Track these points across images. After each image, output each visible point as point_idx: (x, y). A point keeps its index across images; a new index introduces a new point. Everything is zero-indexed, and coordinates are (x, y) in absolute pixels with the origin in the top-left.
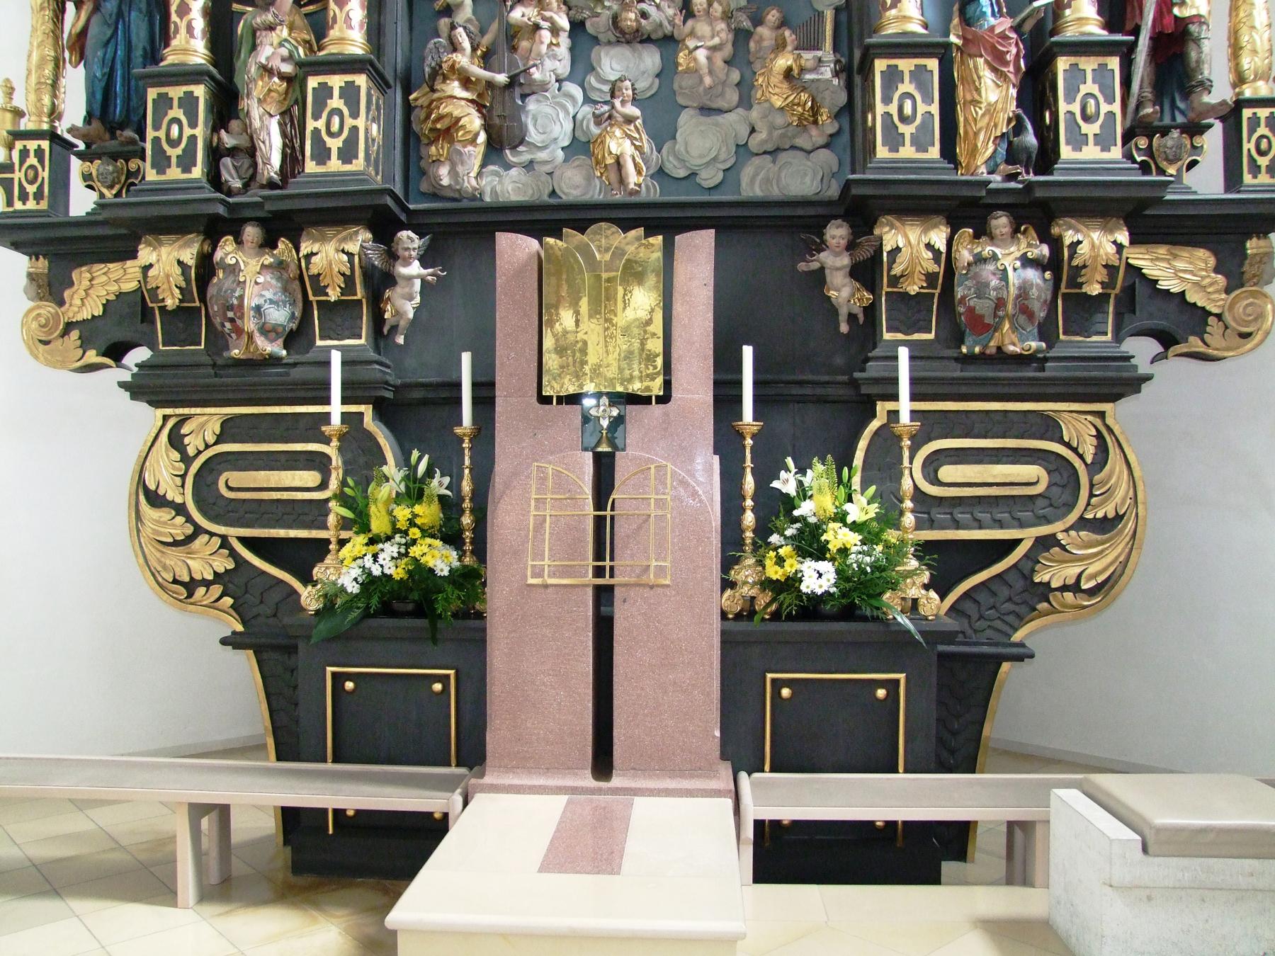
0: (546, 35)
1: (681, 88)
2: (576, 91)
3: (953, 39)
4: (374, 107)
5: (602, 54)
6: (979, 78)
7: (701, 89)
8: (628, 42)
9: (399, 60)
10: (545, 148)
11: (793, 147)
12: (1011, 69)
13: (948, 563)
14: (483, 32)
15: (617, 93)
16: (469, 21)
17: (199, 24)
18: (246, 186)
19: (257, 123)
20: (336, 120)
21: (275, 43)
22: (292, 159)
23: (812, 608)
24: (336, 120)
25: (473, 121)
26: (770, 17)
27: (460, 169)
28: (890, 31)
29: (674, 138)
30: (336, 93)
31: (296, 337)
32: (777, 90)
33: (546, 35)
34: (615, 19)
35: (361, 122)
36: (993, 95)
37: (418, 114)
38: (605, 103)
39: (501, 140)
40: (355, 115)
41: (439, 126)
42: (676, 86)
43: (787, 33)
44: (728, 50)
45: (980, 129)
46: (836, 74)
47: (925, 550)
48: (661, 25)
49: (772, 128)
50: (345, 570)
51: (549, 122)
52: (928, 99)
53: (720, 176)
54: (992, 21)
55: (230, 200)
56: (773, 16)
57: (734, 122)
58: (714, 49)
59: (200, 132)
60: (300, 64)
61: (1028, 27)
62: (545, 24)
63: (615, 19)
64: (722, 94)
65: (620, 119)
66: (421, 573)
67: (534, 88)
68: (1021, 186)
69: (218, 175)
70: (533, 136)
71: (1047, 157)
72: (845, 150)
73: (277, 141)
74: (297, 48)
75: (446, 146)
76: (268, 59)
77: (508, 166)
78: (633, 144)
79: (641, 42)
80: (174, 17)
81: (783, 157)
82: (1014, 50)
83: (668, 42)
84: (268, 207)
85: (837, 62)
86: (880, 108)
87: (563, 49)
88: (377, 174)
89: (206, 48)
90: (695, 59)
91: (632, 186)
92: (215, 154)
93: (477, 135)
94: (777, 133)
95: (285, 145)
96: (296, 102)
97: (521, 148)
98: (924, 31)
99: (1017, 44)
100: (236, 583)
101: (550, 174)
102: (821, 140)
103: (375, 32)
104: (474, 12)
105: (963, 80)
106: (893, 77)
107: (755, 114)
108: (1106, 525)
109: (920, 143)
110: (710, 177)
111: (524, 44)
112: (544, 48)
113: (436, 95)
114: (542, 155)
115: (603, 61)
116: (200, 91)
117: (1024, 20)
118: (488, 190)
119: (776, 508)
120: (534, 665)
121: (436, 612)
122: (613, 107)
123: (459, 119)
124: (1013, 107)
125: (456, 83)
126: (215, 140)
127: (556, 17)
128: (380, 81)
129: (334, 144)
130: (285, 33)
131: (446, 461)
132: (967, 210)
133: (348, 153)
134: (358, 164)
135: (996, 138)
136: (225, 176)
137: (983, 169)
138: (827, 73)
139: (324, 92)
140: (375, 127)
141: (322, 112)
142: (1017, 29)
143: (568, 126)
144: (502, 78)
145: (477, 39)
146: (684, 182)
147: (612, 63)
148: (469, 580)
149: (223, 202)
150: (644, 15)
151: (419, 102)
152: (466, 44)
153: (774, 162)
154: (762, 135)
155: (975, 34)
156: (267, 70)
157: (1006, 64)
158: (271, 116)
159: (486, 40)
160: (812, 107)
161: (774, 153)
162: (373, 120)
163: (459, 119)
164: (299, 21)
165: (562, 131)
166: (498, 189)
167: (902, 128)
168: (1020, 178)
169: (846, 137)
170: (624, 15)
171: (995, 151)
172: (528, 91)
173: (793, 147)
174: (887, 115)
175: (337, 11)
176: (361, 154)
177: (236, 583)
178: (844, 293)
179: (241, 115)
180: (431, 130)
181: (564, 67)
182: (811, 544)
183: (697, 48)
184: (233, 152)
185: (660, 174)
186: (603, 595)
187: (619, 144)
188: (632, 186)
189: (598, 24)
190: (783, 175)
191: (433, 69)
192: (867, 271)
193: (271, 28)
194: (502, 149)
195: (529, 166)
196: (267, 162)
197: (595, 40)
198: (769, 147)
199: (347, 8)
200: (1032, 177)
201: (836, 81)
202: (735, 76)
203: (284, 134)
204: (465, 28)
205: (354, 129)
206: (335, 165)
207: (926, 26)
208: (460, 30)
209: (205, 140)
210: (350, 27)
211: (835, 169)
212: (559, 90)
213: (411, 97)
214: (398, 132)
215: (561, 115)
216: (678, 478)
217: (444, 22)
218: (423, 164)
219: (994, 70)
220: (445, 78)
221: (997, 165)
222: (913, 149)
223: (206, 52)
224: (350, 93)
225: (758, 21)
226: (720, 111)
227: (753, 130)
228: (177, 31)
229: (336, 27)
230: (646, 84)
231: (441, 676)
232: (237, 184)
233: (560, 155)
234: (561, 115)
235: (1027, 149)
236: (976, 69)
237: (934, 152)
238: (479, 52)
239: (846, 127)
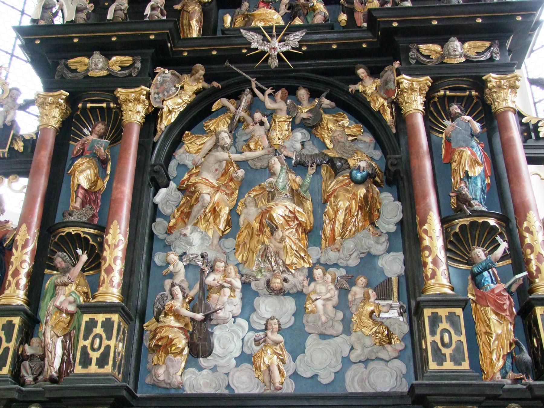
0: (227, 291)
1: (307, 322)
2: (244, 323)
3: (470, 296)
4: (121, 333)
5: (261, 302)
6: (489, 319)
7: (320, 323)
8: (276, 295)
9: (139, 303)
10: (224, 357)
11: (378, 359)
12: (508, 313)
14: (191, 288)
15: (269, 327)
16: (182, 281)
17: (23, 281)
18: (35, 379)
19: (48, 340)
20: (98, 341)
21: (67, 293)
22: (67, 363)
24: (98, 341)
25: (181, 342)
26: (359, 281)
27: (171, 371)
28: (432, 293)
29: (304, 352)
30: (99, 324)
32: (366, 325)
33: (227, 291)
34: (268, 282)
35: (112, 343)
37: (147, 335)
38: (262, 331)
39: (199, 347)
40: (109, 338)
41: (160, 343)
42: (304, 321)
43: (371, 291)
44: (336, 300)
45: (493, 350)
46: (401, 314)
48: (296, 286)
49: (364, 347)
51: (228, 340)
52: (458, 332)
53: (333, 376)
54: (492, 286)
55: (24, 389)
56: (362, 281)
57: (341, 344)
58: (328, 299)
59: (12, 345)
60: (80, 307)
61: (514, 288)
62: (228, 285)
63: (268, 282)
64: (333, 326)
65: (271, 342)
67: (219, 321)
68: (525, 387)
69: (19, 371)
70: (217, 349)
72: (410, 360)
73: (59, 351)
74: (79, 297)
75: (163, 355)
76: (61, 303)
77: (201, 369)
78: (278, 358)
79: (284, 295)
80: (10, 278)
81: (372, 365)
82: (508, 303)
83: (300, 296)
84: (48, 395)
85: (401, 307)
86: (429, 338)
87: (237, 299)
88: (119, 373)
89: (26, 295)
90: (316, 306)
91: (277, 385)
92: (20, 359)
93: (183, 350)
94: (366, 351)
95: (64, 354)
96: (74, 328)
97: (209, 358)
98: (450, 292)
99: (509, 299)
101: (227, 374)
102: (395, 354)
103: (127, 288)
104: (186, 276)
105: (478, 319)
106: (435, 320)
107: (353, 338)
109: (457, 359)
110: (326, 378)
111: (215, 296)
112: (225, 299)
113: (160, 325)
114: (222, 362)
115: (261, 306)
116: (16, 321)
117: (511, 285)
118: (188, 383)
122: (266, 336)
123: (172, 340)
124: (512, 337)
125: (173, 318)
126: (21, 349)
127: (234, 281)
128: (126, 317)
129: (95, 356)
130: (73, 288)
133: (102, 362)
134: (108, 369)
135: (504, 356)
136: (23, 372)
137: (498, 376)
138: (394, 313)
139: (92, 324)
140: (121, 345)
141: (89, 336)
142: (508, 290)
143: (239, 344)
144: (199, 316)
145: (187, 291)
146: (309, 381)
147: (266, 307)
149: (20, 391)
150: (286, 280)
151: (149, 328)
152: (180, 295)
153: (366, 368)
154: (358, 351)
155: (483, 294)
156: (60, 310)
157: (505, 310)
158: (58, 337)
159: (193, 293)
160: (388, 335)
161: (366, 362)
162: (120, 341)
163: (172, 340)
164: (82, 281)
166: (194, 383)
167: (444, 350)
168: (523, 381)
169: (409, 352)
170: (274, 280)
171: (505, 364)
172: (215, 323)
173: (378, 359)
174: (434, 343)
175: (106, 276)
176: (111, 363)
179: (40, 335)
180: (155, 345)
181: (237, 310)
183: (317, 299)
184: (31, 358)
185: (295, 376)
187: (269, 358)
188: (277, 385)
189: (258, 285)
190: (371, 376)
191: (159, 309)
193: (65, 285)
194: (198, 357)
195: (214, 369)
196: (51, 365)
197: (257, 294)
198: (363, 358)
199: (112, 275)
200: (531, 381)
201: (401, 319)
202: (340, 315)
203: (64, 348)
204: (180, 286)
205: (108, 347)
206: (93, 368)
207: (453, 289)
208: (177, 287)
209: (14, 350)
210: (112, 286)
211: (404, 371)
212: (234, 322)
213: (144, 325)
214: (135, 346)
215: (235, 338)
217: (168, 283)
218: (148, 366)
219: (497, 314)
220: (166, 315)
221: (507, 373)
222: (452, 363)
223: (25, 297)
224: (108, 325)
225: (352, 283)
226: (332, 336)
227: (352, 348)
228: (9, 285)
229: (104, 286)
230: (287, 321)
232: (29, 378)
233: (234, 362)
234: (235, 338)
235: (525, 363)
236: (486, 314)
237: (465, 366)
238: (187, 300)
239: (410, 346)
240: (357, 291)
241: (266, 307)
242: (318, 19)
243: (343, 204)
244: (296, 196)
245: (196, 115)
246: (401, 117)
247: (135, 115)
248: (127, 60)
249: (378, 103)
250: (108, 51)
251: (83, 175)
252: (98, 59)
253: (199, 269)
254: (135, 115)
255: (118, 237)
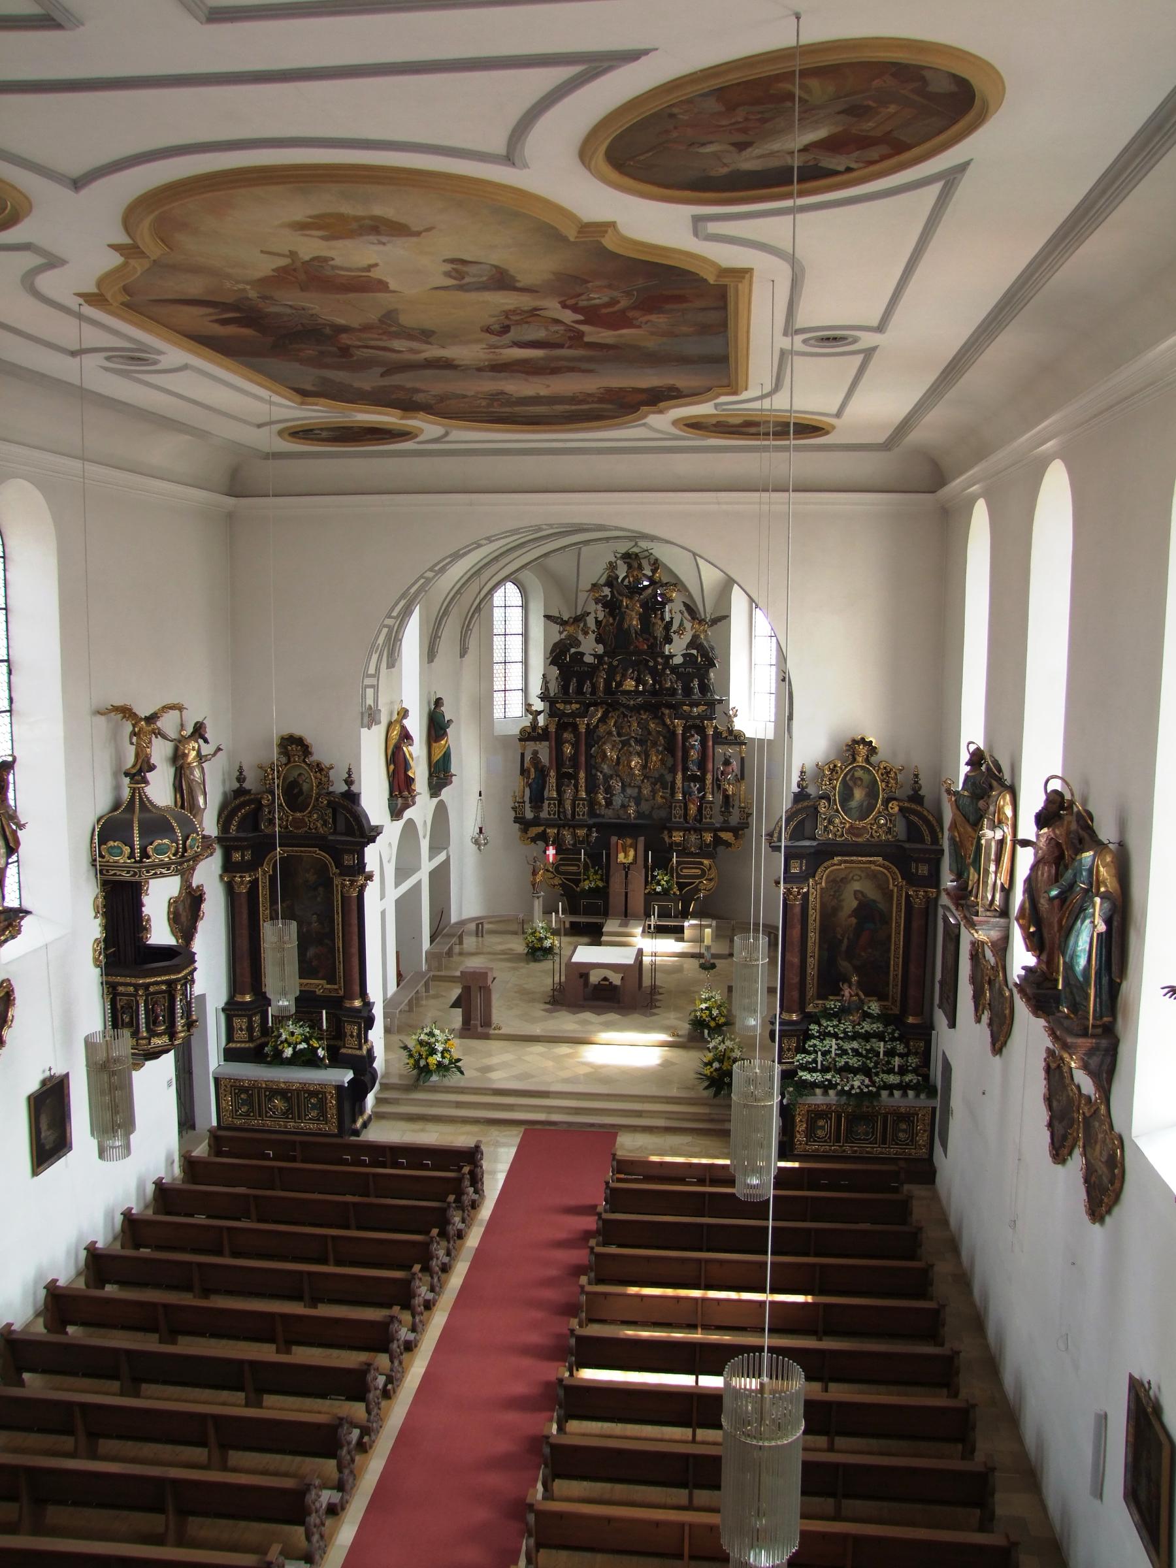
13: (681, 886)
23: (659, 893)
25: (603, 802)
31: (574, 845)
36: (693, 809)
47: (677, 883)
50: (586, 885)
51: (618, 801)
66: (597, 886)
71: (700, 821)
83: (640, 788)
100: (562, 885)
108: (710, 880)
119: (653, 877)
120: (616, 900)
121: (602, 893)
131: (601, 868)
132: (687, 830)
148: (607, 887)
165: (620, 802)
177: (562, 885)
178: (667, 839)
182: (658, 884)
186: (626, 893)
192: (671, 837)
216: (638, 877)
231: (600, 902)
240: (658, 786)
241: (629, 791)
242: (648, 687)
243: (654, 758)
244: (639, 754)
245: (603, 720)
246: (674, 734)
247: (582, 729)
248: (578, 706)
249: (668, 721)
250: (571, 703)
251: (568, 750)
252: (568, 706)
253: (607, 778)
254: (582, 729)
255: (582, 775)
